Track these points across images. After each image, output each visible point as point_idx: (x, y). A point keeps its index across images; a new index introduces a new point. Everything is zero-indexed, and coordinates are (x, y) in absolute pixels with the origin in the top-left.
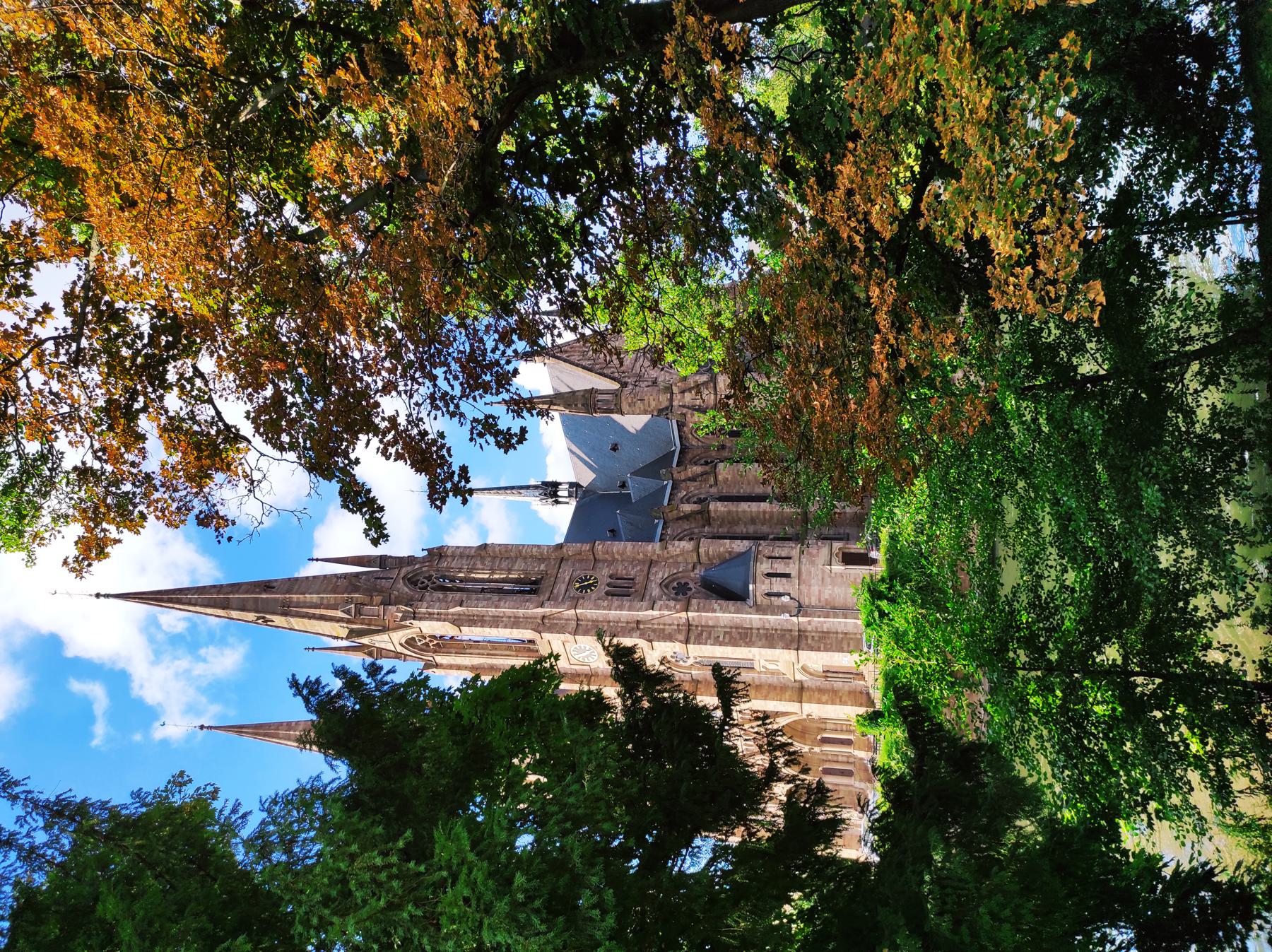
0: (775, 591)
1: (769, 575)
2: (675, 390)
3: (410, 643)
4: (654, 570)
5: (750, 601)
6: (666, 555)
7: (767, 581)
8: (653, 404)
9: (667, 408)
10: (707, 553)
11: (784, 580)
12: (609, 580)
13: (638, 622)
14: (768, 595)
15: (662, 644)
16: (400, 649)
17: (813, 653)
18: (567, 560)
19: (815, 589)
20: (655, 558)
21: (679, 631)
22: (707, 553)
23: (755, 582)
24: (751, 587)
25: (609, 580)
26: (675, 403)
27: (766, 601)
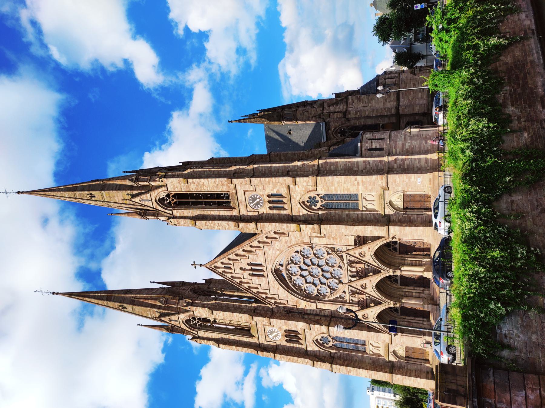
0: (374, 147)
1: (370, 139)
3: (161, 201)
5: (358, 154)
7: (369, 142)
11: (380, 141)
13: (288, 171)
14: (370, 150)
15: (301, 178)
16: (156, 206)
17: (397, 176)
19: (400, 143)
21: (312, 173)
23: (361, 142)
24: (359, 144)
27: (368, 153)
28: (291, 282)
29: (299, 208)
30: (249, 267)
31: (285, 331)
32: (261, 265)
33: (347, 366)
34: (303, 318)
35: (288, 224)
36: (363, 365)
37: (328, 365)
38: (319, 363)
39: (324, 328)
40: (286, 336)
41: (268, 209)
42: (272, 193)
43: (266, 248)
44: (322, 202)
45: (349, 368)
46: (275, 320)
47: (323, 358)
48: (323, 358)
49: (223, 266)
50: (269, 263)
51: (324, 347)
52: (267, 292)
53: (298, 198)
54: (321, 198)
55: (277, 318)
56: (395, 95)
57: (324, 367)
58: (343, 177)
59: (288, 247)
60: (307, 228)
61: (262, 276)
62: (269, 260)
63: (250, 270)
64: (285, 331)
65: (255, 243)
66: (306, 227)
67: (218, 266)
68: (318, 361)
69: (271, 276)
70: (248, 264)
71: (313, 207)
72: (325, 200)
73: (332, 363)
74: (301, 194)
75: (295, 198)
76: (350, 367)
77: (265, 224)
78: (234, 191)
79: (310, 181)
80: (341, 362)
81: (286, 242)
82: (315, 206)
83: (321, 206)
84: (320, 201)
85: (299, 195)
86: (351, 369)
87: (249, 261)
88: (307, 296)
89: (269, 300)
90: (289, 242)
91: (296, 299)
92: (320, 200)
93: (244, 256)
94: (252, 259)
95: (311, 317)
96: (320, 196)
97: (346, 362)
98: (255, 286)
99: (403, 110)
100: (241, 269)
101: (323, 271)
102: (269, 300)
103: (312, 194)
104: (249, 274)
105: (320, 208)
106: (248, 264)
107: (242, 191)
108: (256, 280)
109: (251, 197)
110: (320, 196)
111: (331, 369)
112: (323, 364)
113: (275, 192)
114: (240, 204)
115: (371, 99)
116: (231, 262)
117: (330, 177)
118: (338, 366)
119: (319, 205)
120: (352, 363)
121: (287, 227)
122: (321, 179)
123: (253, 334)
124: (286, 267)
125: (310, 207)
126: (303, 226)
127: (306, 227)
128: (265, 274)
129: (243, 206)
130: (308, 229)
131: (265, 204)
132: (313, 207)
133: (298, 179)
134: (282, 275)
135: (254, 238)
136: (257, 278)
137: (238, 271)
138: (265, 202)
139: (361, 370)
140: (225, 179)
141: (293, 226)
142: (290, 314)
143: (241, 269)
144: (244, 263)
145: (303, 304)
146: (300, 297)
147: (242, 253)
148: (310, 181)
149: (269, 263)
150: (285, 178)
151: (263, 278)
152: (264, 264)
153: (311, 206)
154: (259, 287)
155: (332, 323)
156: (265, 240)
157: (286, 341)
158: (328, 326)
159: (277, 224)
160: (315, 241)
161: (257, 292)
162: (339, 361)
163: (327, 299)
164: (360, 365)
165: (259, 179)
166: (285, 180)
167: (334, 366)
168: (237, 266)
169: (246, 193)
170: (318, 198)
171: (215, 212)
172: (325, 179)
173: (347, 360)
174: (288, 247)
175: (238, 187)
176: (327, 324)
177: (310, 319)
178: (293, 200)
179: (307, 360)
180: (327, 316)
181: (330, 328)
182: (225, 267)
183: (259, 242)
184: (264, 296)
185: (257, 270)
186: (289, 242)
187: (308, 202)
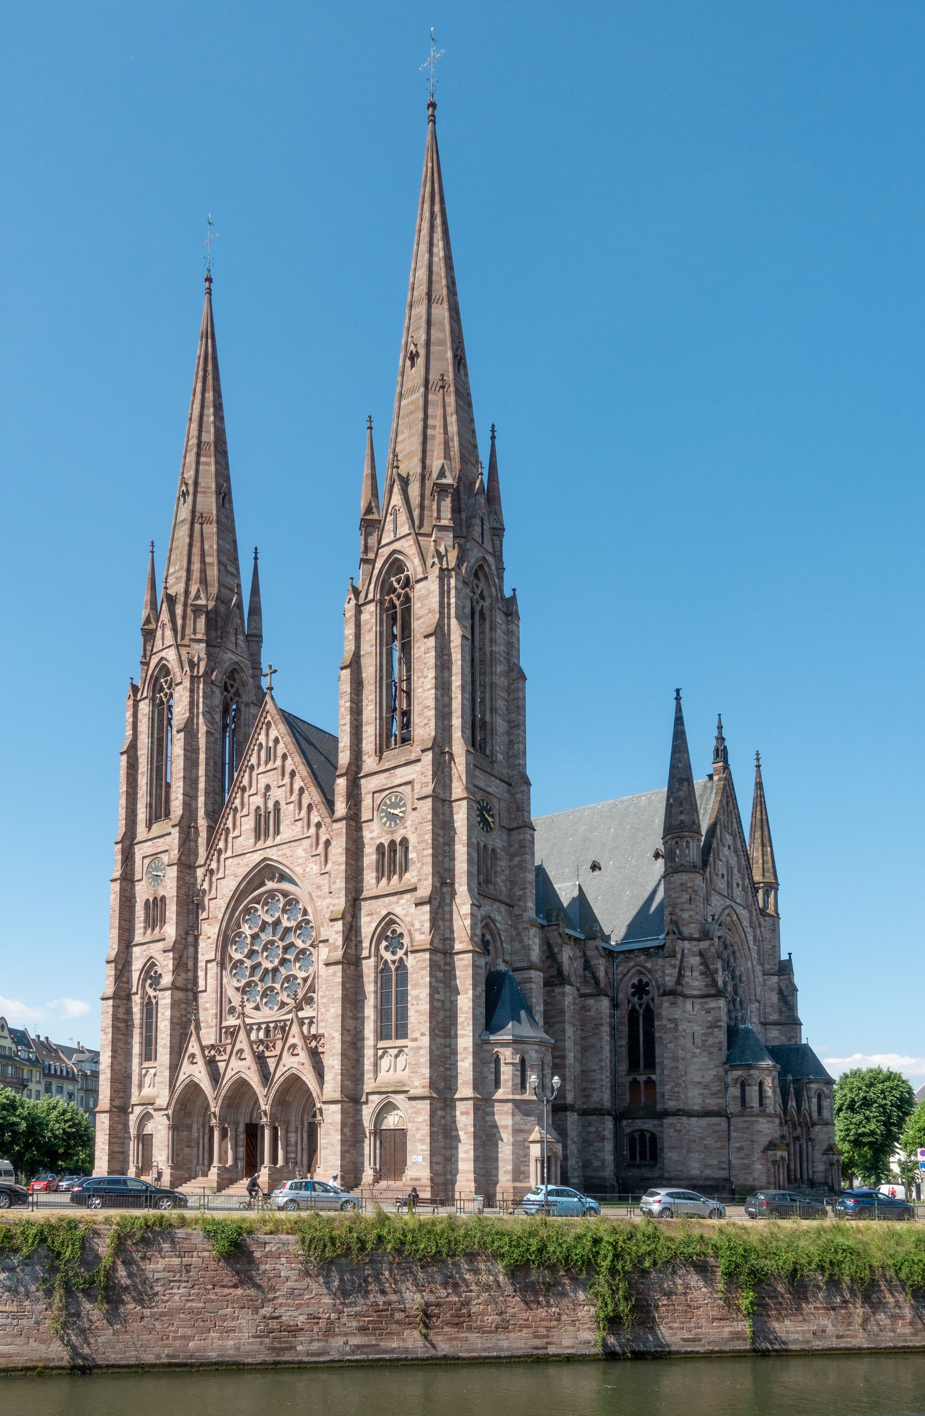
2: (704, 945)
4: (503, 908)
6: (521, 927)
8: (686, 915)
9: (680, 933)
10: (529, 980)
12: (490, 847)
15: (428, 917)
18: (509, 792)
20: (517, 911)
22: (529, 980)
25: (490, 847)
26: (687, 944)
28: (250, 902)
29: (378, 913)
30: (271, 805)
31: (163, 898)
32: (277, 832)
33: (113, 1026)
34: (187, 934)
35: (344, 892)
36: (120, 1058)
37: (110, 991)
38: (113, 972)
39: (167, 980)
40: (155, 898)
41: (378, 842)
42: (410, 848)
43: (306, 843)
44: (394, 962)
45: (110, 1030)
46: (175, 874)
47: (125, 979)
48: (125, 979)
49: (271, 744)
50: (280, 853)
51: (145, 980)
52: (229, 854)
53: (398, 910)
54: (401, 959)
55: (179, 879)
56: (716, 1108)
57: (108, 982)
58: (427, 1007)
59: (310, 893)
60: (334, 933)
61: (257, 838)
62: (285, 851)
63: (266, 808)
64: (163, 898)
65: (315, 818)
66: (337, 932)
67: (271, 731)
68: (116, 969)
69: (257, 857)
70: (277, 803)
71: (384, 943)
72: (397, 969)
73: (115, 997)
74: (404, 915)
75: (398, 902)
76: (113, 1033)
77: (344, 840)
78: (413, 757)
79: (423, 937)
80: (121, 1016)
81: (319, 887)
82: (387, 948)
83: (386, 961)
84: (394, 958)
85: (404, 912)
86: (110, 1036)
87: (283, 806)
88: (227, 939)
89: (215, 858)
90: (320, 893)
91: (220, 917)
92: (396, 958)
93: (292, 792)
94: (288, 811)
95: (191, 949)
96: (404, 957)
97: (122, 1025)
98: (238, 823)
99: (672, 1125)
100: (268, 788)
101: (275, 970)
102: (215, 858)
103: (406, 941)
104: (258, 808)
105: (382, 958)
106: (277, 803)
107: (414, 776)
108: (248, 824)
109: (401, 800)
110: (404, 957)
111: (106, 996)
112: (112, 979)
113: (412, 855)
114: (387, 774)
115: (710, 1053)
116: (279, 762)
117: (428, 979)
118: (111, 1010)
119: (388, 956)
120: (122, 1037)
121: (340, 889)
122: (424, 960)
123: (154, 827)
124: (277, 890)
125: (382, 936)
126: (339, 925)
127: (337, 932)
128: (260, 845)
129: (384, 781)
130: (334, 936)
131: (387, 833)
132: (384, 943)
133: (427, 908)
134: (263, 884)
135: (324, 811)
136: (253, 825)
137: (263, 781)
138: (392, 832)
139: (110, 1054)
140: (433, 733)
141: (340, 903)
142: (191, 903)
143: (268, 788)
144: (277, 794)
145: (210, 931)
146: (224, 924)
147: (296, 787)
148: (423, 937)
149: (280, 853)
150: (430, 877)
151: (252, 841)
152: (278, 840)
153: (387, 938)
154: (237, 833)
155: (180, 995)
156: (323, 839)
157: (148, 900)
158: (174, 987)
159: (343, 867)
160: (323, 953)
161: (228, 828)
162: (122, 1010)
163: (225, 981)
164: (120, 1051)
165: (430, 817)
166: (426, 879)
167: (111, 1002)
168: (271, 779)
169: (410, 786)
170: (400, 953)
171: (370, 712)
172: (424, 968)
173: (127, 1026)
174: (310, 893)
175: (417, 767)
176: (177, 984)
177: (186, 948)
178: (395, 898)
179: (116, 946)
180: (196, 983)
181: (169, 992)
182: (269, 749)
183: (318, 825)
184: (221, 845)
185: (266, 824)
186: (320, 893)
187: (394, 931)
